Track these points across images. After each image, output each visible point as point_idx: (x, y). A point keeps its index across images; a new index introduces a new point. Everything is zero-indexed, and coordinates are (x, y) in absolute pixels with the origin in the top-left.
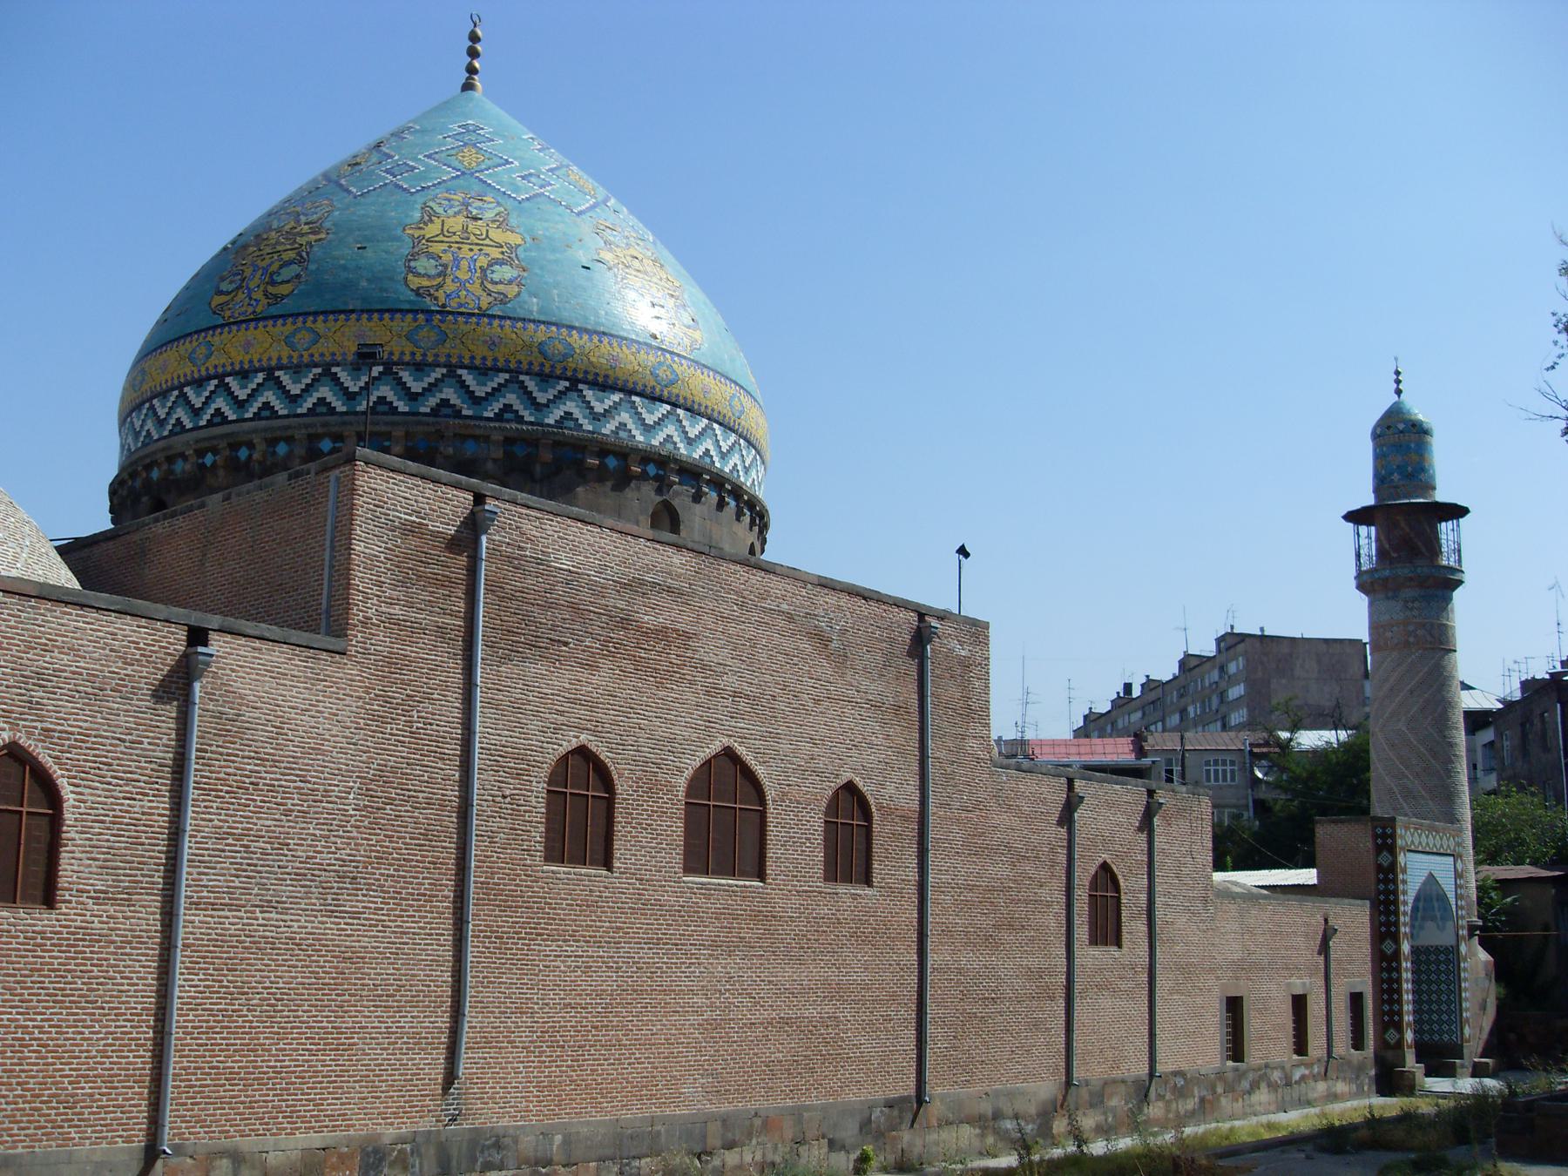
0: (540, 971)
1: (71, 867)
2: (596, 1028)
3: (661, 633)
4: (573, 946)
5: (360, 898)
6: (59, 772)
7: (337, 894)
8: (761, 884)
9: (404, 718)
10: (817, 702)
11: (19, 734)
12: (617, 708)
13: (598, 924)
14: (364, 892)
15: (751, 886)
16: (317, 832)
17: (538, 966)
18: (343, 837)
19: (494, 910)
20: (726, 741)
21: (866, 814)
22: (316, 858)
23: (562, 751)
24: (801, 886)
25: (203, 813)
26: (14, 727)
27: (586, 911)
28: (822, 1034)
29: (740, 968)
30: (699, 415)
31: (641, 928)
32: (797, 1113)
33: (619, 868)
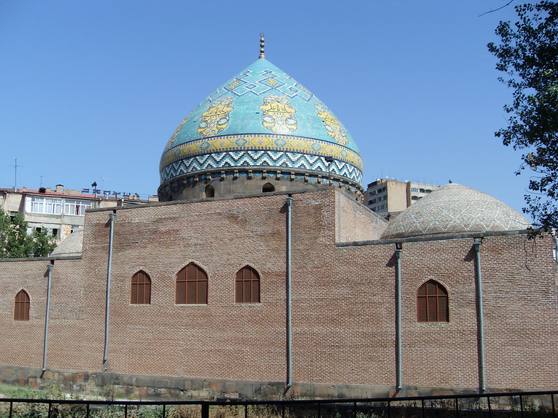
0: (129, 333)
1: (32, 312)
2: (146, 349)
3: (168, 232)
8: (206, 305)
10: (231, 240)
15: (201, 306)
20: (191, 261)
21: (258, 276)
23: (135, 273)
24: (223, 305)
28: (235, 356)
29: (197, 333)
30: (221, 152)
32: (224, 382)
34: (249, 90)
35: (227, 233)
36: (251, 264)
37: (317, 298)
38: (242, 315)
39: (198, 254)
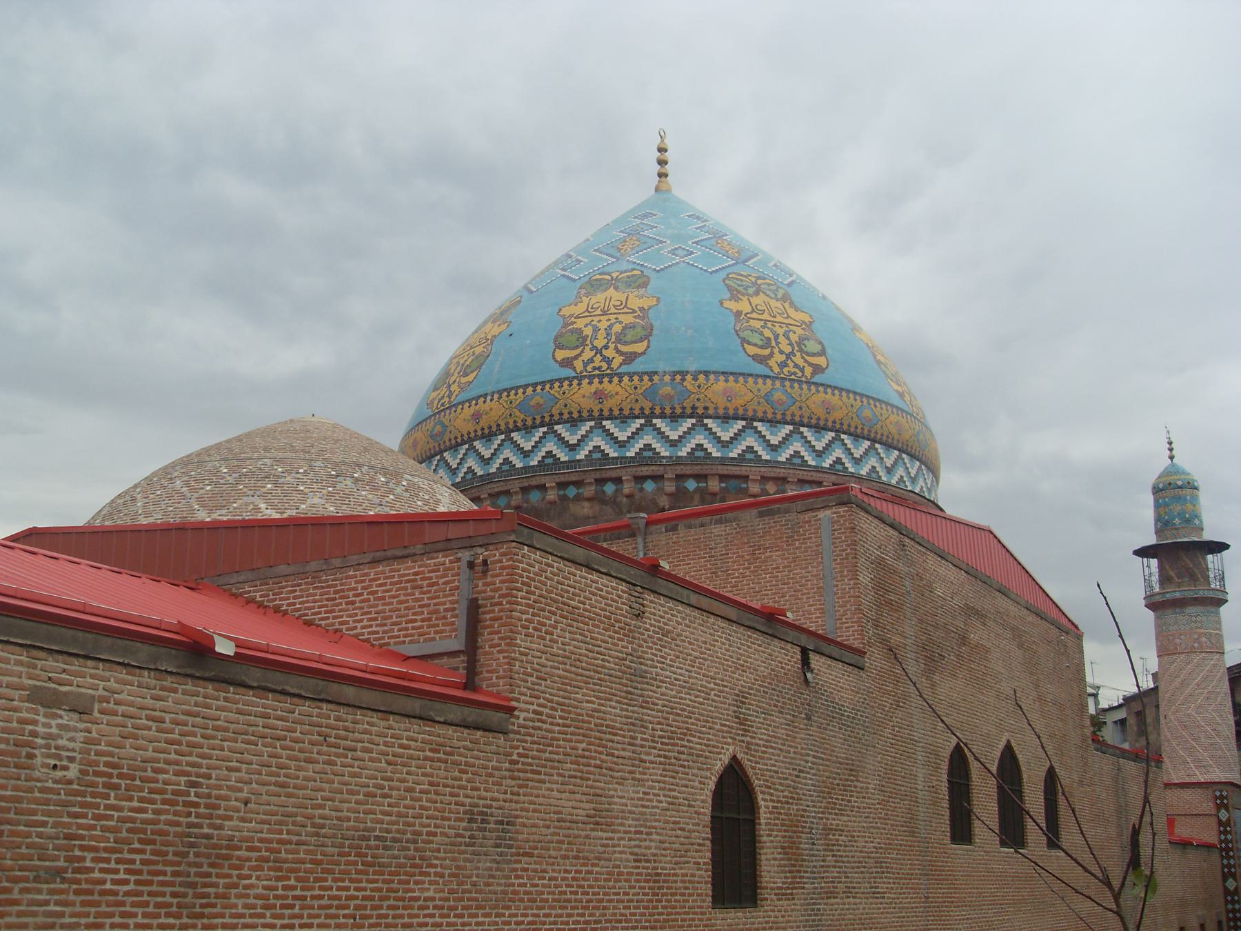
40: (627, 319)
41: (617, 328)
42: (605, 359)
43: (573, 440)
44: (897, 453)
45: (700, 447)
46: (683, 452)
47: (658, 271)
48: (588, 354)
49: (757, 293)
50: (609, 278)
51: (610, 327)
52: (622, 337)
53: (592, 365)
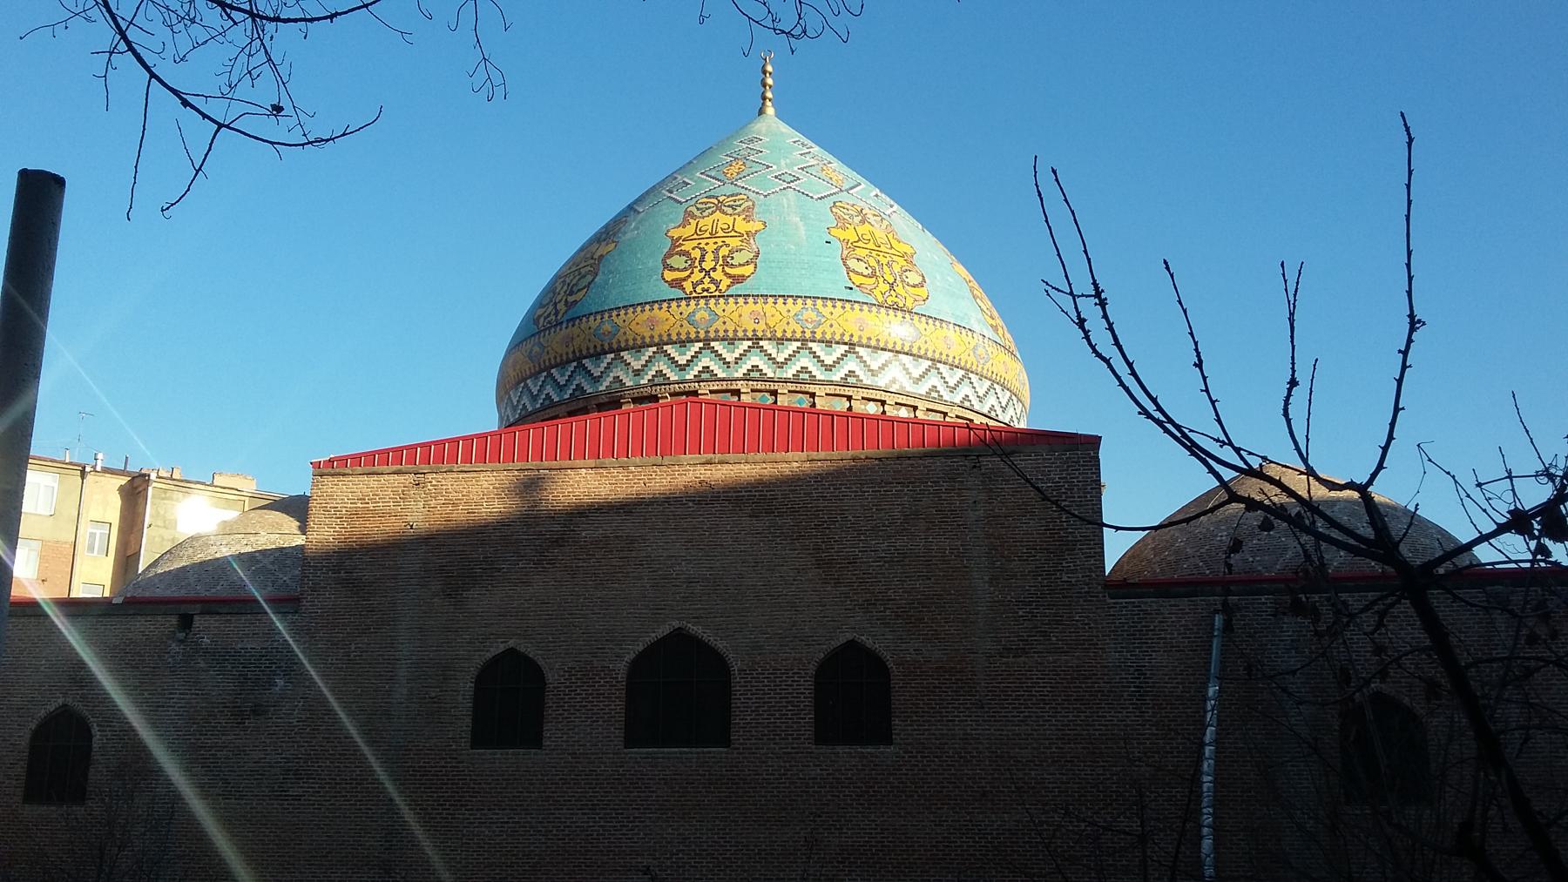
0: (464, 835)
4: (498, 814)
5: (302, 785)
6: (91, 719)
7: (282, 783)
8: (726, 750)
9: (342, 651)
11: (67, 699)
12: (550, 613)
13: (526, 794)
14: (305, 780)
15: (710, 753)
16: (268, 741)
17: (462, 831)
18: (289, 742)
19: (420, 788)
20: (676, 624)
22: (265, 758)
23: (489, 656)
25: (185, 735)
26: (65, 695)
27: (513, 783)
31: (574, 796)
33: (548, 746)
34: (785, 185)
35: (787, 552)
36: (863, 637)
37: (1060, 733)
38: (836, 779)
39: (699, 606)
40: (734, 242)
41: (724, 251)
42: (713, 281)
43: (682, 360)
44: (989, 383)
45: (804, 369)
46: (789, 372)
47: (766, 196)
48: (697, 276)
49: (863, 222)
50: (716, 202)
51: (716, 251)
52: (729, 259)
53: (700, 286)
